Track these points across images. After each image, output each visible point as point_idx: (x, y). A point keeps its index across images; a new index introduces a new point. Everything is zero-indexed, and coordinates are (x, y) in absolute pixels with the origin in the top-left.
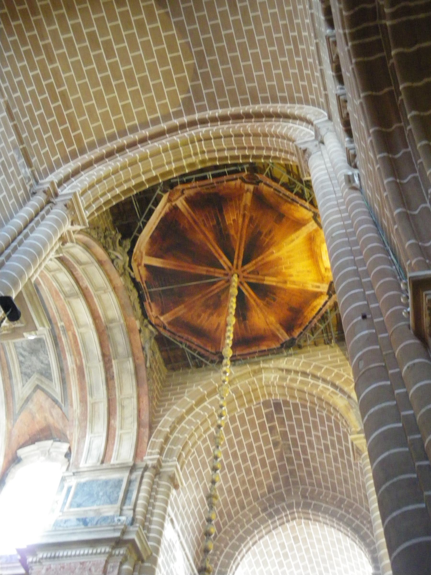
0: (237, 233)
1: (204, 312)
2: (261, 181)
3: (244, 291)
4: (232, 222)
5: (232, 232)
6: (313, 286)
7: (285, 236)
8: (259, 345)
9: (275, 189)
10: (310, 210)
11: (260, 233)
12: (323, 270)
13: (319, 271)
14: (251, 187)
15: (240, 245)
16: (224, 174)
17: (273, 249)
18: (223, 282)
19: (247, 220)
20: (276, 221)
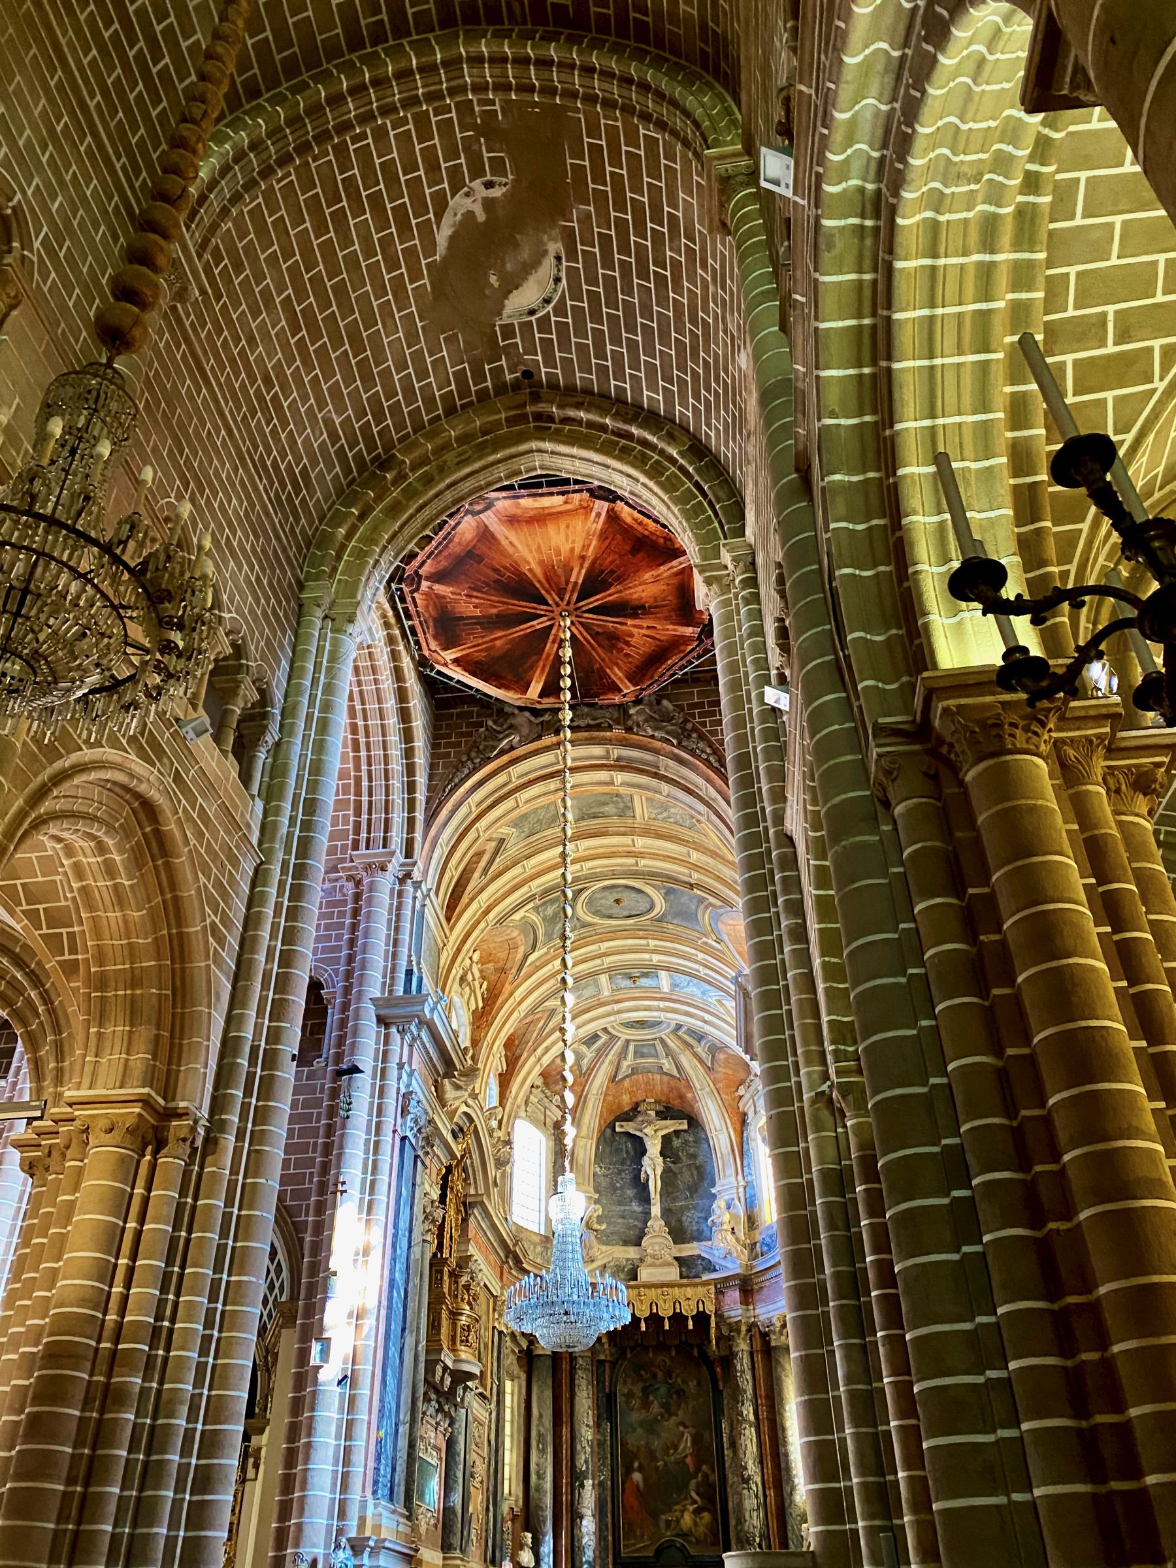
1: (621, 650)
2: (416, 572)
5: (494, 611)
7: (504, 553)
11: (496, 581)
12: (569, 507)
13: (567, 512)
14: (425, 585)
16: (406, 610)
17: (525, 569)
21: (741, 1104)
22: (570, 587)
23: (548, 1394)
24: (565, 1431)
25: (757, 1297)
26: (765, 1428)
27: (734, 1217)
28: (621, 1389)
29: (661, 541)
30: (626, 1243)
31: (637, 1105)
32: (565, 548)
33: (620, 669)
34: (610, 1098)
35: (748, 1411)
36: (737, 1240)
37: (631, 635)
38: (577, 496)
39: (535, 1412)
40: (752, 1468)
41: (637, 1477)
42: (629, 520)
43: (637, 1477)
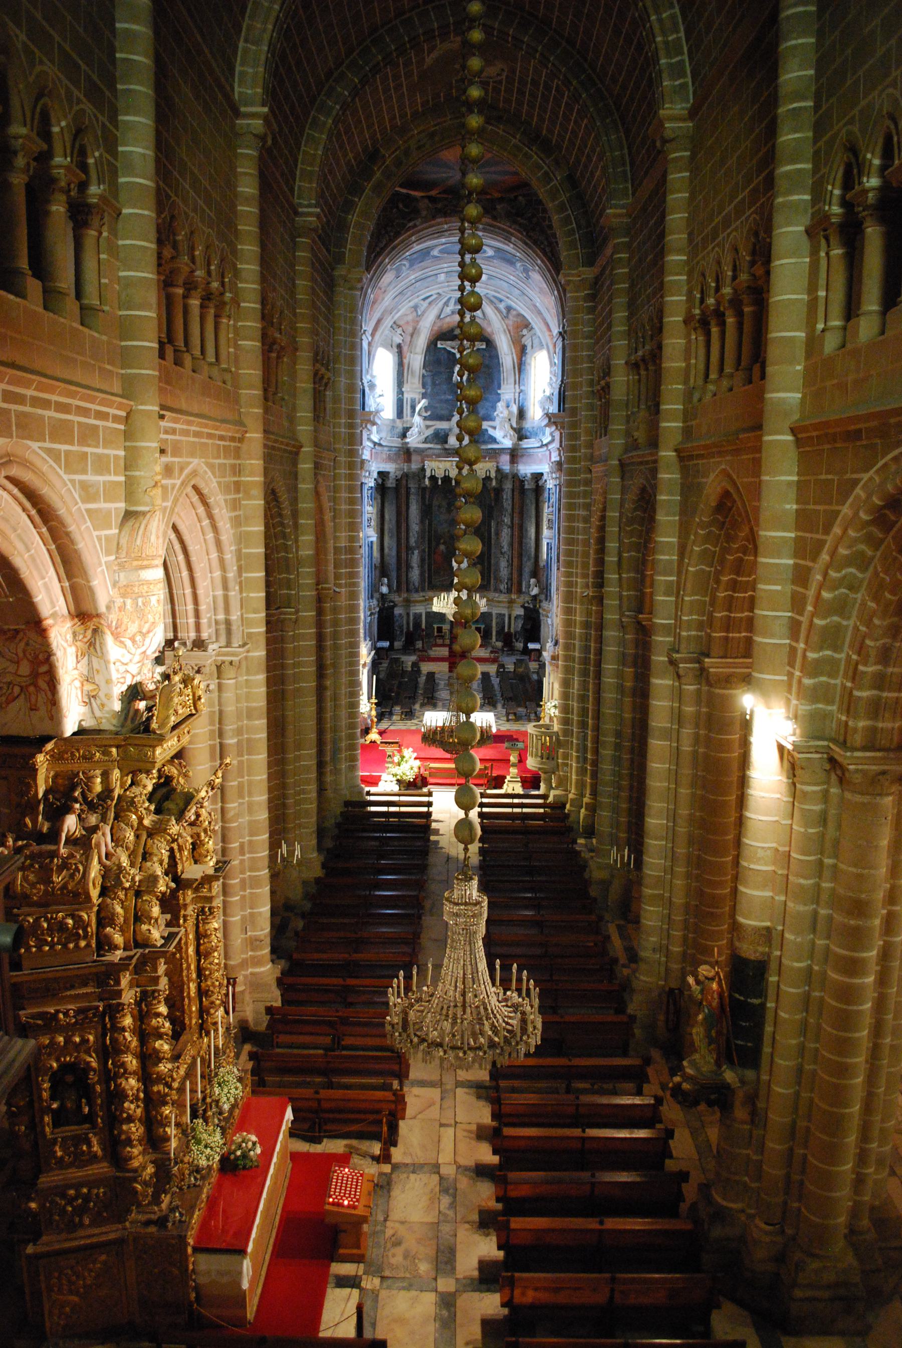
21: (523, 340)
23: (394, 508)
24: (404, 526)
25: (520, 460)
26: (516, 529)
27: (510, 413)
28: (435, 503)
30: (440, 418)
31: (452, 330)
34: (436, 328)
35: (507, 520)
36: (512, 427)
39: (387, 517)
40: (506, 548)
41: (442, 547)
43: (442, 547)
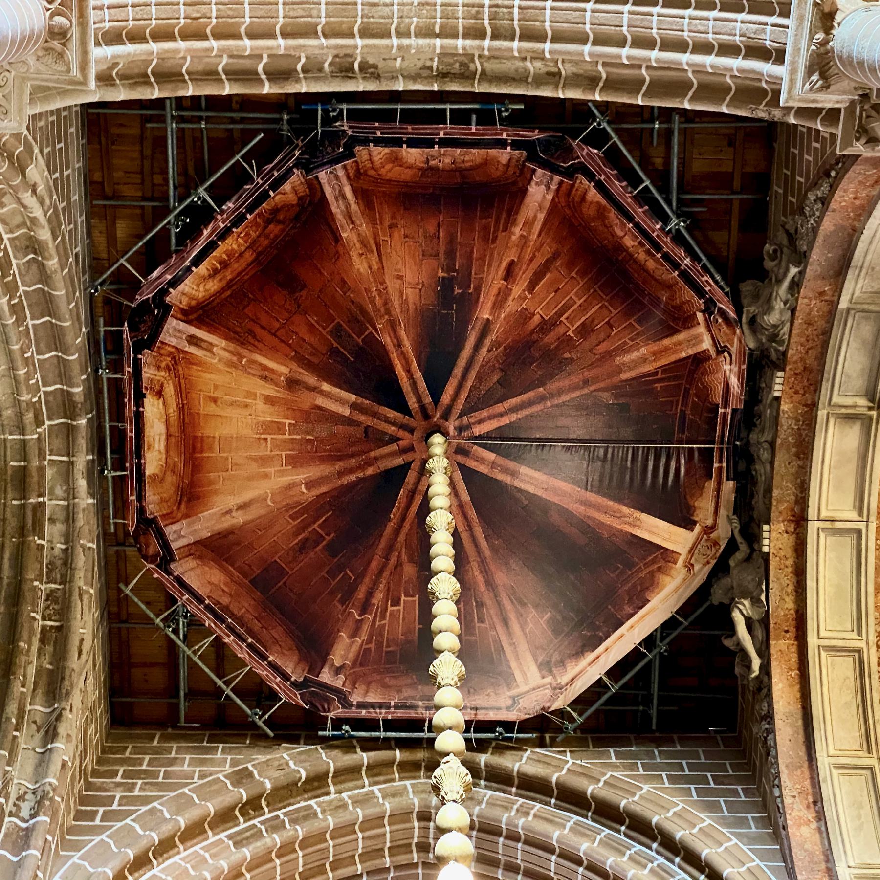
0: (399, 565)
1: (566, 342)
3: (422, 385)
4: (403, 598)
6: (209, 348)
7: (262, 526)
8: (428, 170)
9: (264, 658)
10: (179, 580)
11: (332, 550)
12: (169, 390)
14: (326, 676)
15: (397, 531)
16: (390, 725)
17: (308, 495)
18: (478, 430)
19: (361, 594)
20: (282, 572)
22: (362, 418)
29: (274, 229)
32: (266, 414)
33: (624, 350)
37: (525, 316)
38: (148, 373)
42: (213, 286)
